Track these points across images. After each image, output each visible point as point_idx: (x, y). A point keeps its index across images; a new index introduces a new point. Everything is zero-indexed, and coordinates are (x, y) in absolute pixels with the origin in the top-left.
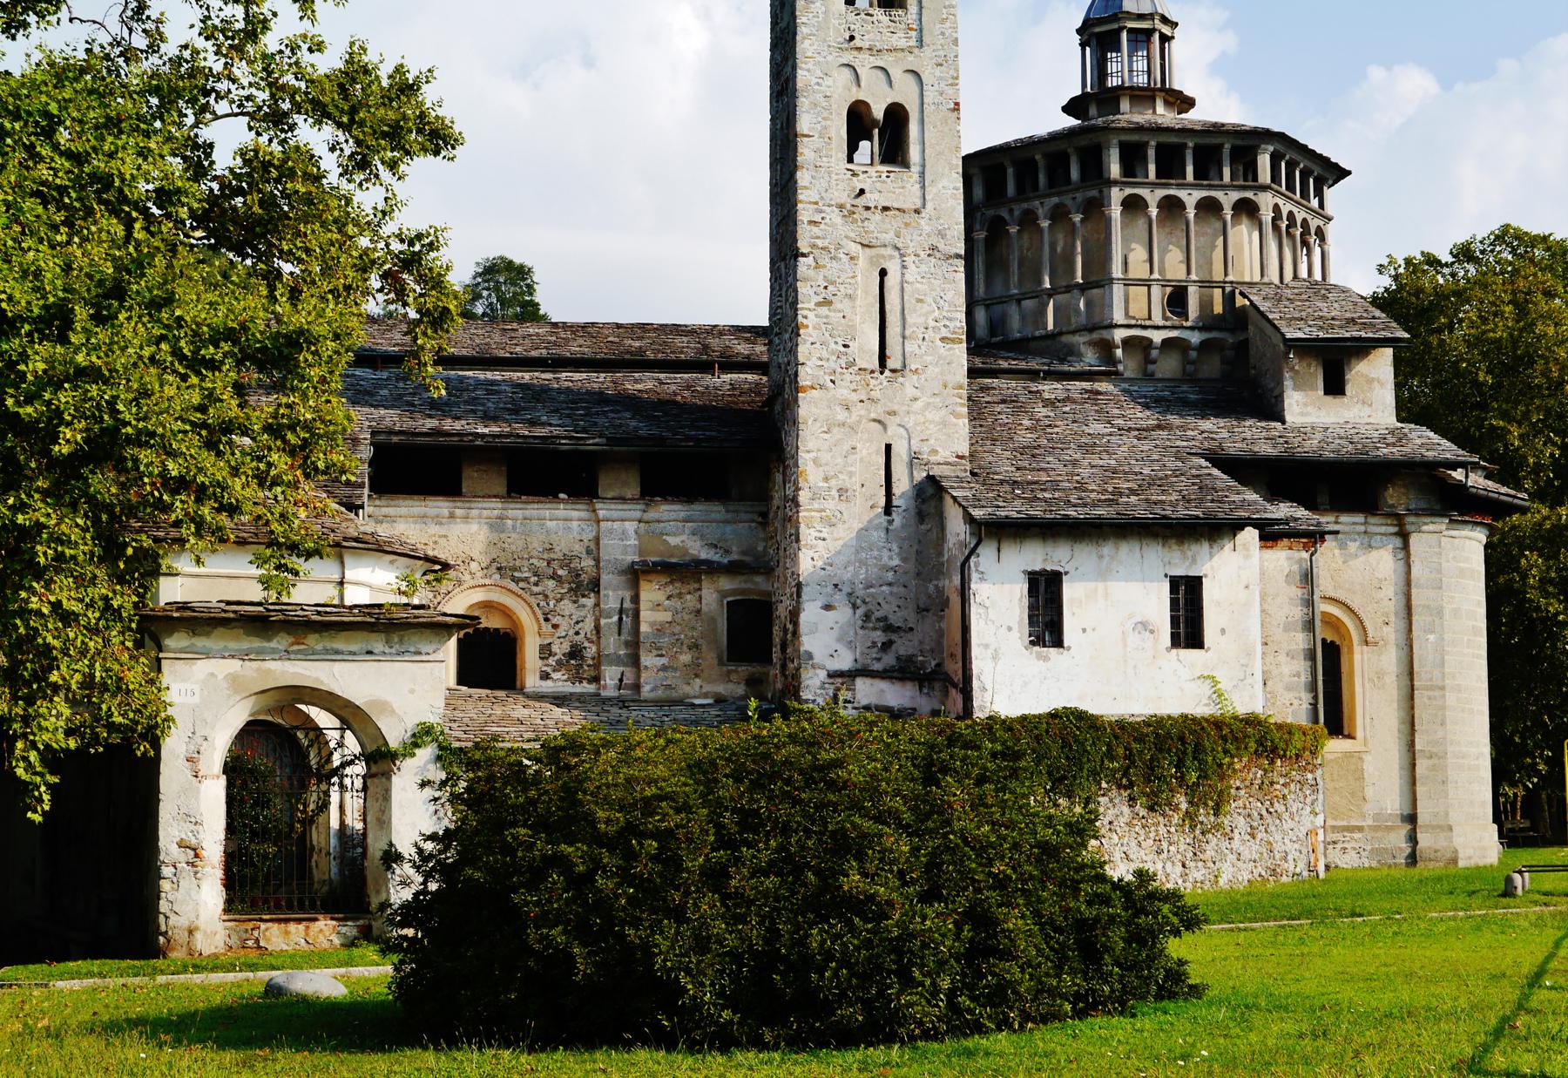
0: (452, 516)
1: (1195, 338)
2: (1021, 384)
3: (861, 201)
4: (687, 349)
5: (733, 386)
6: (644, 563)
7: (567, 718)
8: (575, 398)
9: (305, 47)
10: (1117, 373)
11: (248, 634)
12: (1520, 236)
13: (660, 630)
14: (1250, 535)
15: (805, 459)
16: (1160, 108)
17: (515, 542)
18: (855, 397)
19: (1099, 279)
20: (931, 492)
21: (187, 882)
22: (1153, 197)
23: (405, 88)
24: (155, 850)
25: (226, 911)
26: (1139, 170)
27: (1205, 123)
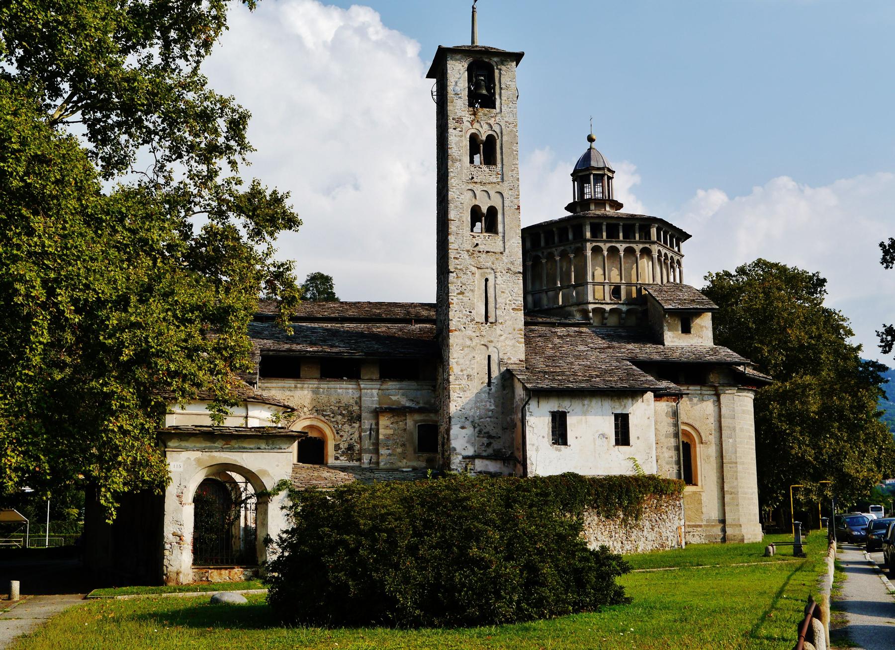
0: (296, 387)
1: (624, 308)
2: (548, 328)
3: (477, 249)
4: (400, 313)
5: (420, 330)
6: (381, 408)
7: (347, 477)
8: (350, 334)
9: (234, 182)
10: (590, 324)
11: (205, 440)
12: (766, 263)
13: (388, 438)
14: (650, 395)
15: (452, 362)
16: (608, 208)
17: (324, 398)
18: (474, 335)
19: (582, 282)
20: (508, 376)
21: (176, 551)
22: (605, 247)
23: (277, 200)
24: (163, 537)
25: (193, 564)
26: (599, 235)
27: (628, 215)
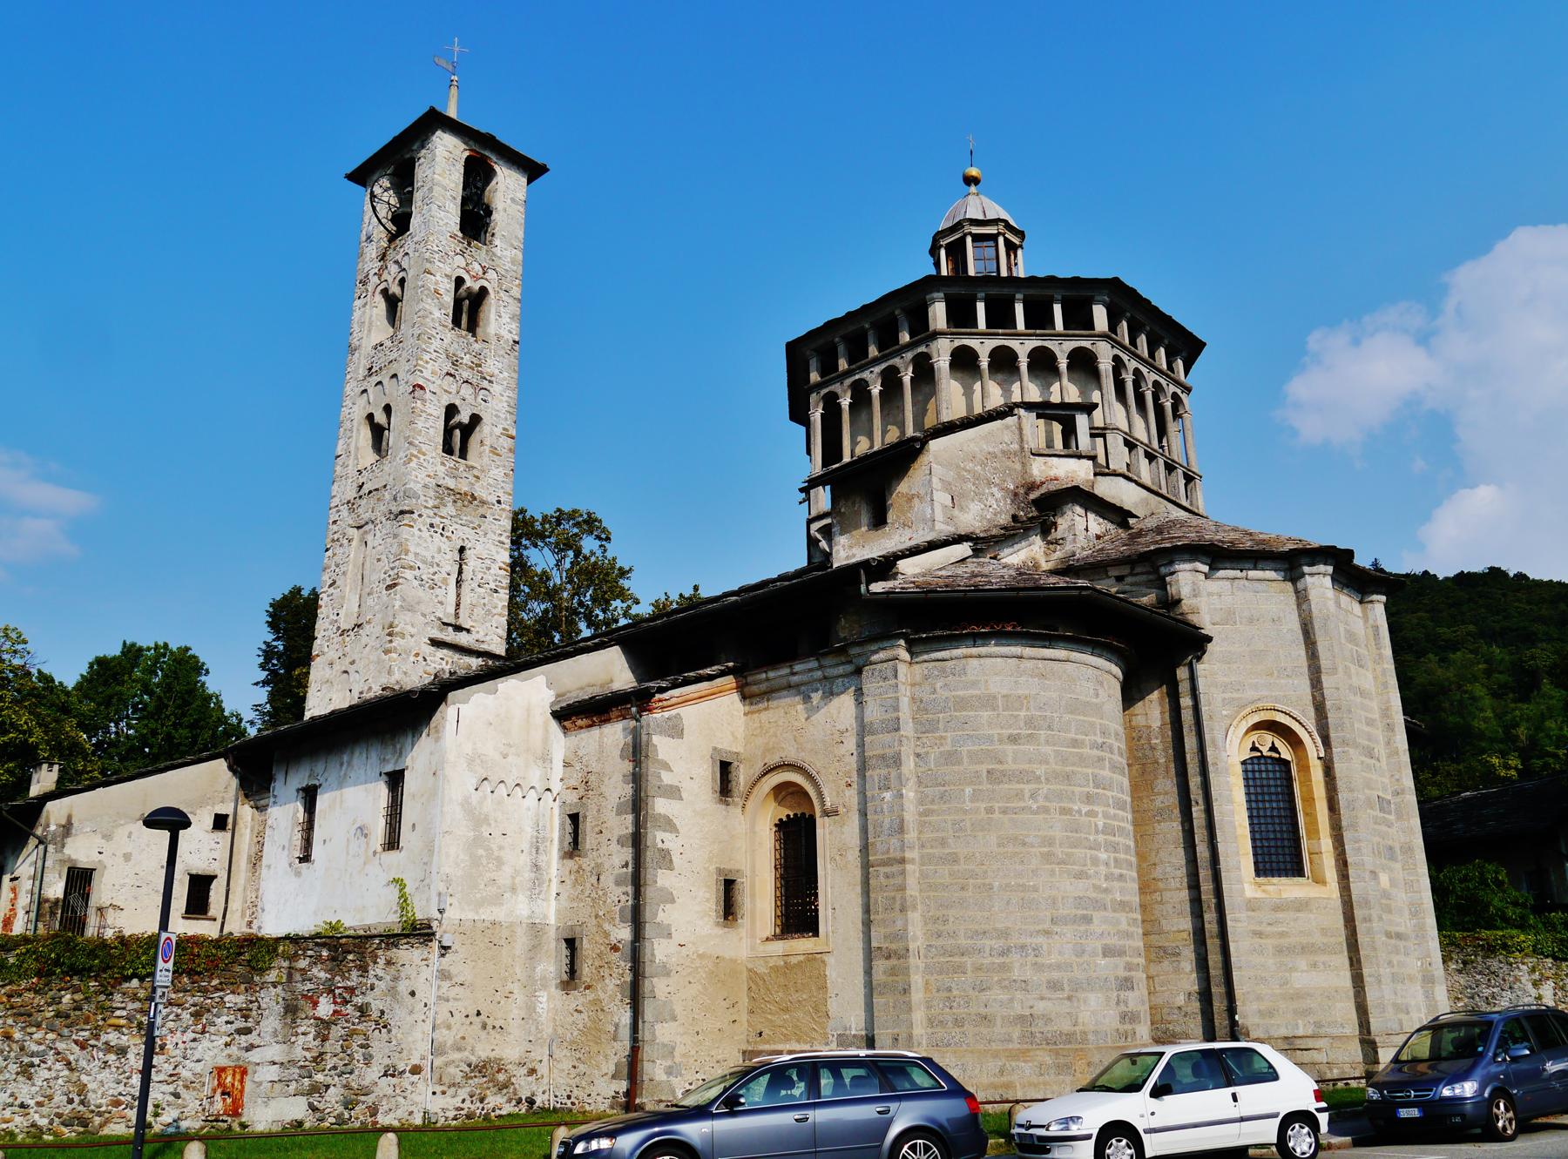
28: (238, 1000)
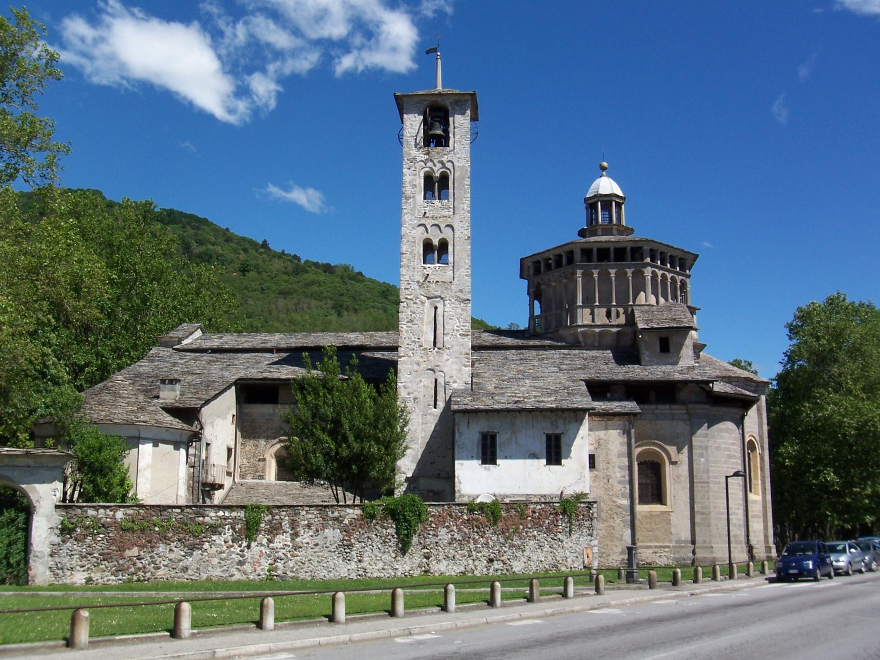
18: (422, 360)
28: (587, 524)
